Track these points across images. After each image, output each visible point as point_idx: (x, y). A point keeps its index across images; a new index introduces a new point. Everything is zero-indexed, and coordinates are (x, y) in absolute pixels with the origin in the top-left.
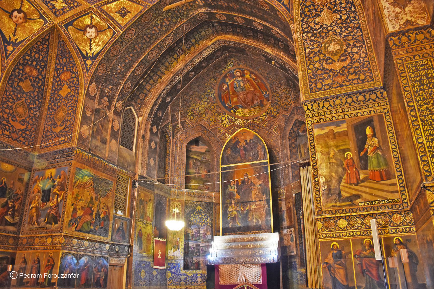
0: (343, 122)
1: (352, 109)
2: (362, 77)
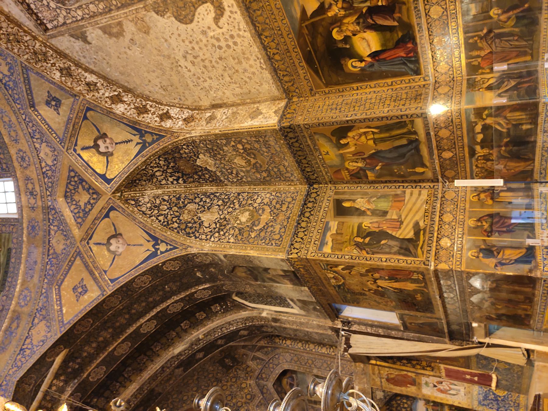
0: (327, 223)
1: (318, 213)
2: (289, 200)
